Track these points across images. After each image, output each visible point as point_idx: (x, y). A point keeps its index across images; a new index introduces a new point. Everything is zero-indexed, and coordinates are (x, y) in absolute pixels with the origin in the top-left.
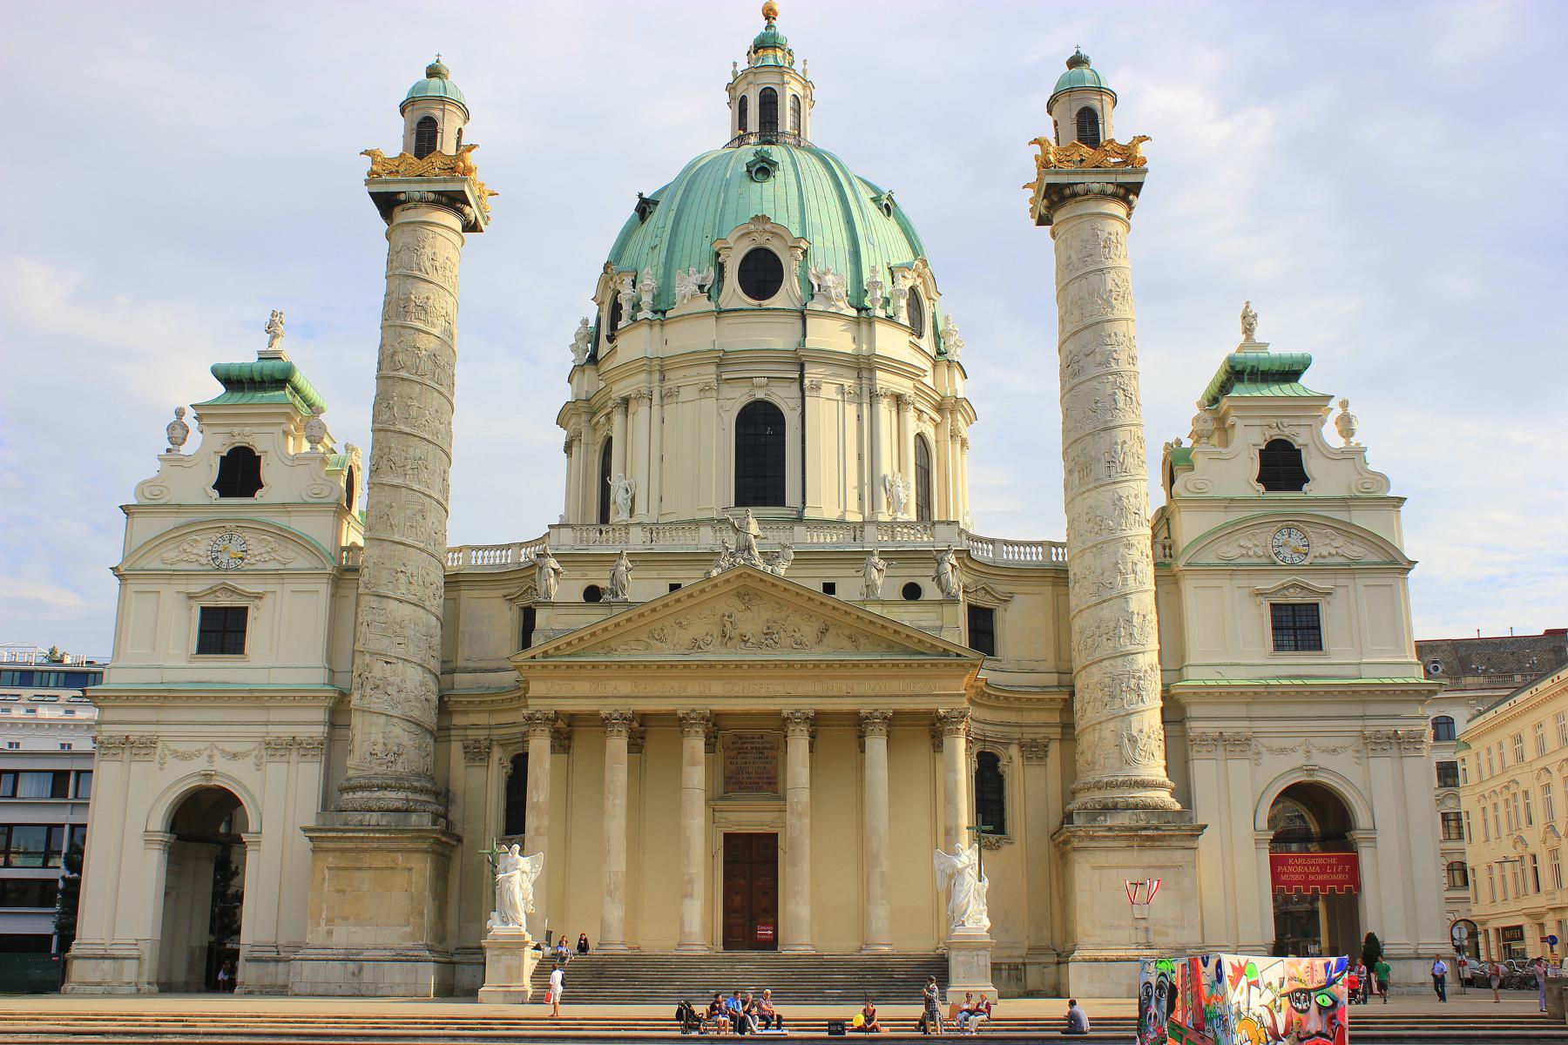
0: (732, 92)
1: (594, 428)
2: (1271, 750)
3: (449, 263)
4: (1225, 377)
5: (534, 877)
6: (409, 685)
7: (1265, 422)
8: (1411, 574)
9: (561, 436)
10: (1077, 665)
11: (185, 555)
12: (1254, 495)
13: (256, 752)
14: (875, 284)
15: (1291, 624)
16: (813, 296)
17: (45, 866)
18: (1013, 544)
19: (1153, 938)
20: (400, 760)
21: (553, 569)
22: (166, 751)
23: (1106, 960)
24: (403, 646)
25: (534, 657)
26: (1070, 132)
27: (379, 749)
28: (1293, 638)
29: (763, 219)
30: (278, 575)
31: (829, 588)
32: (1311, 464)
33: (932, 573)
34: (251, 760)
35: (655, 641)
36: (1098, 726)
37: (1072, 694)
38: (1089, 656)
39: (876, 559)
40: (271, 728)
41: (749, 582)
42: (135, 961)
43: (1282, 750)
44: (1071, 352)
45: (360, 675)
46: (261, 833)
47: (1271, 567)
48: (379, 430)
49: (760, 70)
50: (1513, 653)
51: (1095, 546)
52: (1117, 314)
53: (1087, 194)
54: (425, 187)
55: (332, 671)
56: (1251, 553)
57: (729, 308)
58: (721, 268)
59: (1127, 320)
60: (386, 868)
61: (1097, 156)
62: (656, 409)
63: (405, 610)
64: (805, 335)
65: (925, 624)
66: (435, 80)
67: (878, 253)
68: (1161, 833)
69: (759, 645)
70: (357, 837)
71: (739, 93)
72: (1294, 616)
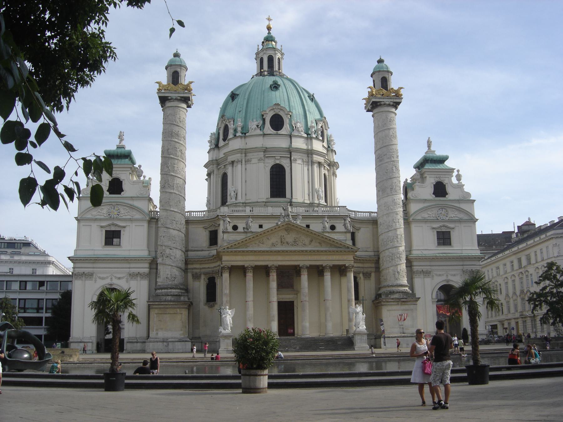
0: (257, 55)
1: (219, 169)
2: (437, 275)
4: (423, 161)
5: (232, 316)
6: (178, 256)
7: (435, 176)
8: (477, 223)
9: (205, 171)
10: (381, 249)
11: (99, 214)
12: (432, 198)
13: (126, 277)
14: (313, 127)
15: (442, 237)
16: (293, 130)
17: (38, 312)
18: (360, 212)
19: (405, 331)
20: (177, 279)
22: (96, 277)
23: (392, 337)
25: (224, 249)
26: (379, 84)
27: (169, 276)
28: (442, 241)
29: (278, 105)
30: (131, 220)
31: (308, 226)
32: (449, 189)
33: (343, 224)
34: (125, 280)
35: (260, 244)
37: (379, 258)
39: (326, 219)
41: (289, 226)
42: (91, 344)
43: (440, 275)
44: (379, 154)
47: (437, 220)
48: (164, 174)
49: (267, 49)
50: (493, 239)
51: (385, 214)
52: (393, 143)
53: (384, 105)
54: (177, 95)
55: (149, 251)
56: (431, 216)
57: (267, 133)
58: (264, 120)
59: (396, 144)
60: (174, 313)
61: (388, 93)
62: (243, 165)
63: (175, 233)
64: (291, 143)
65: (341, 239)
66: (177, 58)
67: (312, 115)
68: (407, 300)
69: (292, 245)
71: (260, 55)
72: (443, 235)
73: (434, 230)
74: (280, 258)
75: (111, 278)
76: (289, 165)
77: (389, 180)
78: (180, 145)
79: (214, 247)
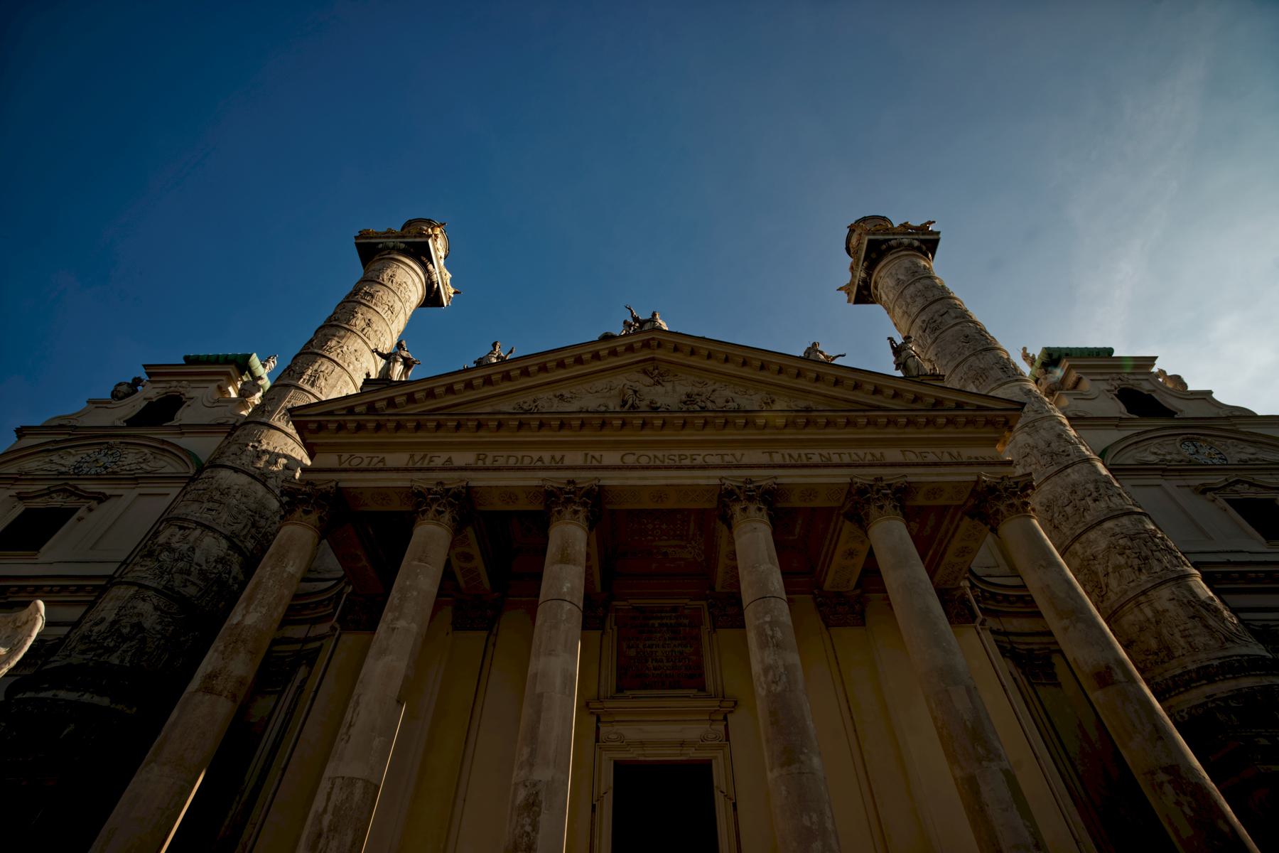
3: (404, 285)
6: (198, 556)
21: (402, 357)
24: (214, 513)
25: (331, 413)
27: (102, 627)
30: (135, 480)
36: (1142, 599)
38: (1077, 523)
41: (659, 354)
73: (1210, 495)
74: (611, 458)
77: (984, 353)
78: (371, 310)
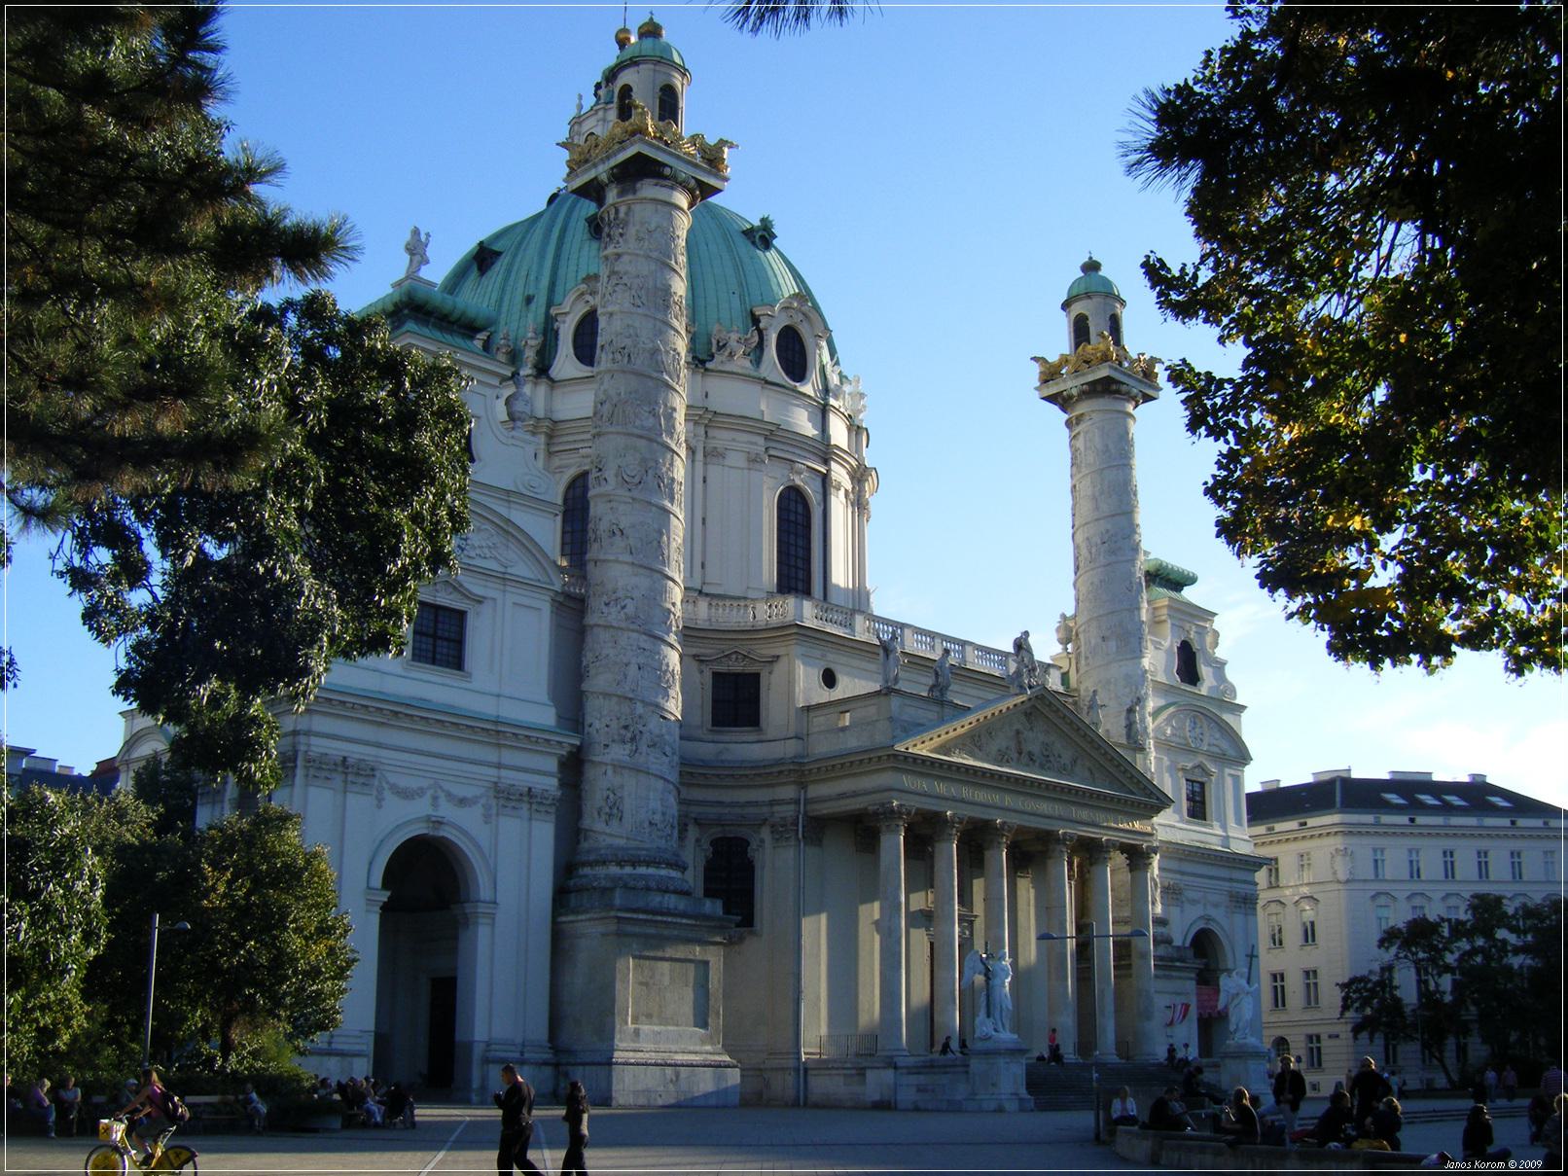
8: (1247, 769)
13: (483, 801)
22: (386, 786)
27: (658, 818)
30: (504, 579)
34: (477, 810)
40: (504, 773)
44: (1107, 531)
45: (626, 727)
46: (495, 903)
58: (760, 333)
70: (662, 922)
75: (435, 798)
76: (820, 497)
79: (746, 734)
